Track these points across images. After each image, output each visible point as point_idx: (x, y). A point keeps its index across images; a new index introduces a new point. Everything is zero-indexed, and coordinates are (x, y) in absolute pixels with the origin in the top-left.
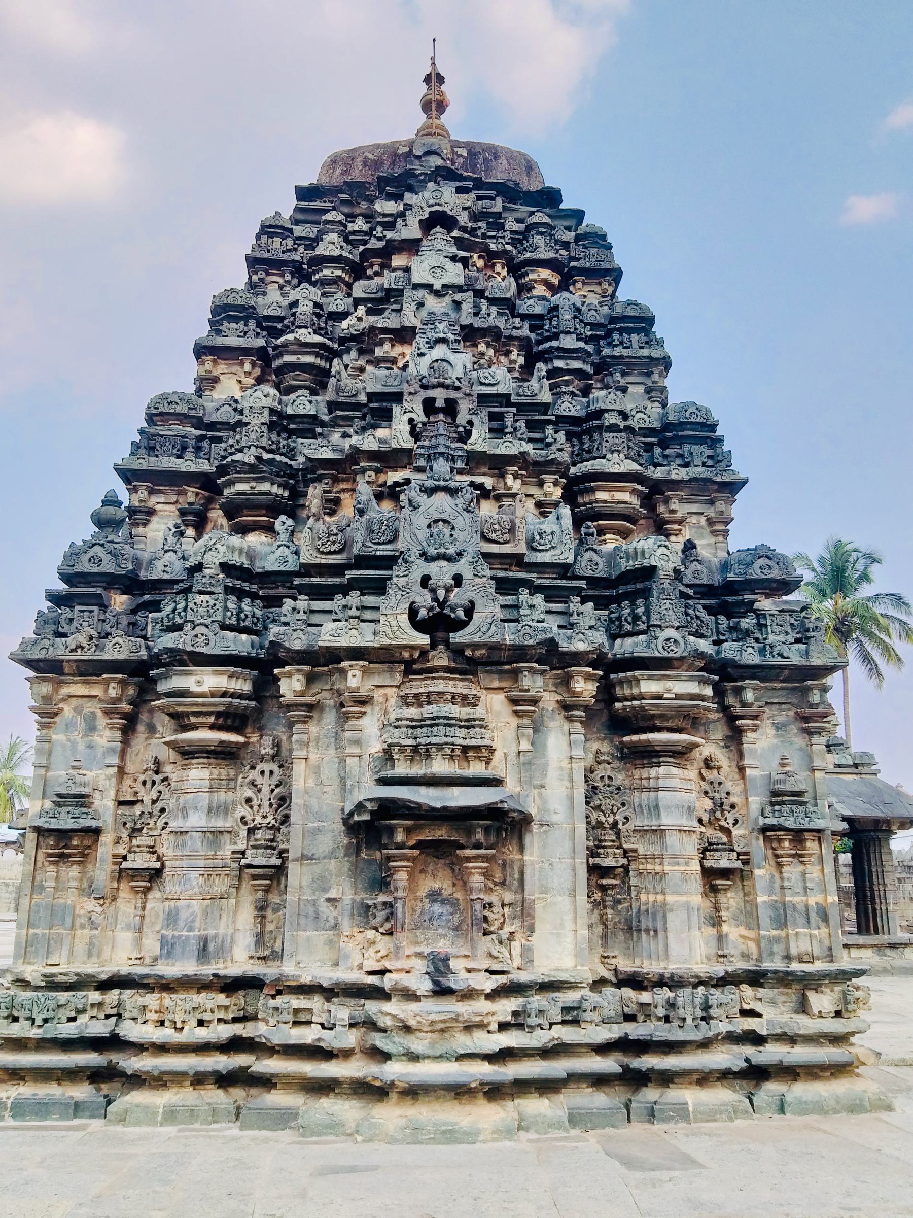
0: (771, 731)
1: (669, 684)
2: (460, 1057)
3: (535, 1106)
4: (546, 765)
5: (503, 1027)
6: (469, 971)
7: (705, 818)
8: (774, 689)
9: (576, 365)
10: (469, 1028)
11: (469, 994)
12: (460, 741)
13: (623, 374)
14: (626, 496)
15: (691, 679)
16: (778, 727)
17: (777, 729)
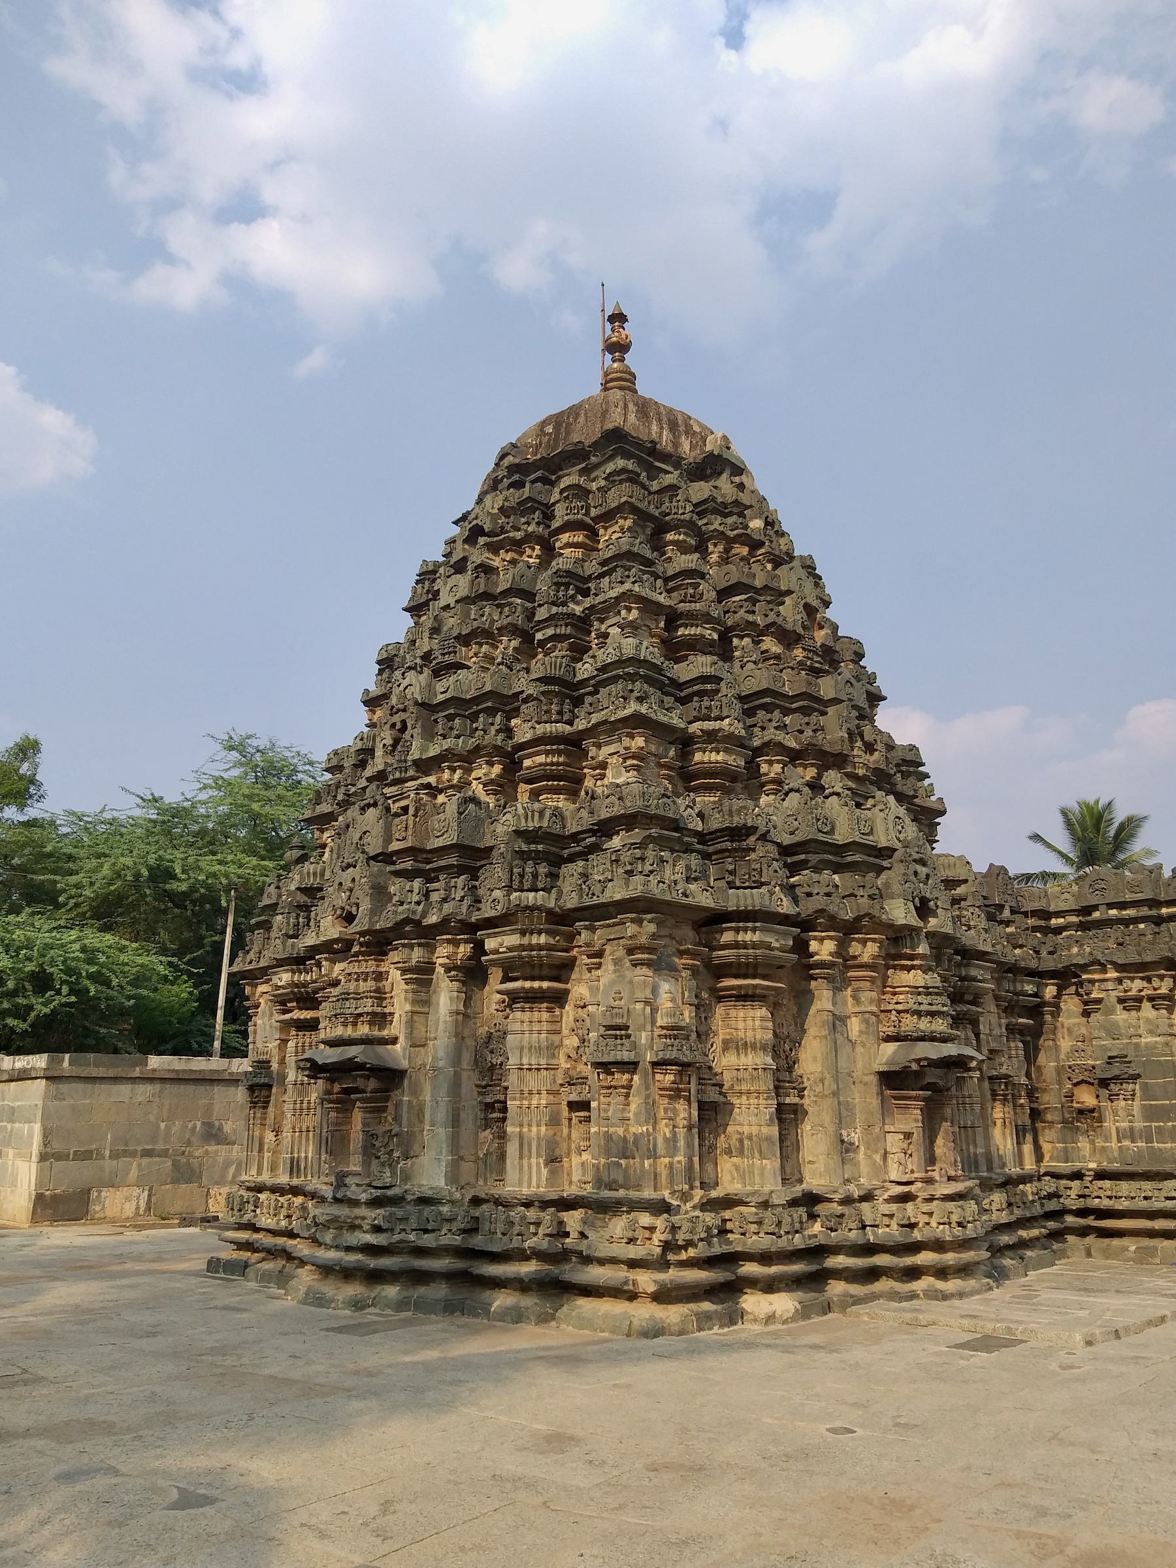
0: (611, 967)
1: (499, 939)
2: (348, 1249)
3: (392, 1291)
4: (438, 1020)
5: (377, 1229)
6: (357, 1185)
7: (574, 1055)
8: (609, 926)
9: (550, 632)
10: (353, 1227)
11: (354, 1203)
12: (352, 1010)
13: (602, 621)
14: (541, 759)
15: (513, 932)
16: (616, 962)
17: (615, 964)
